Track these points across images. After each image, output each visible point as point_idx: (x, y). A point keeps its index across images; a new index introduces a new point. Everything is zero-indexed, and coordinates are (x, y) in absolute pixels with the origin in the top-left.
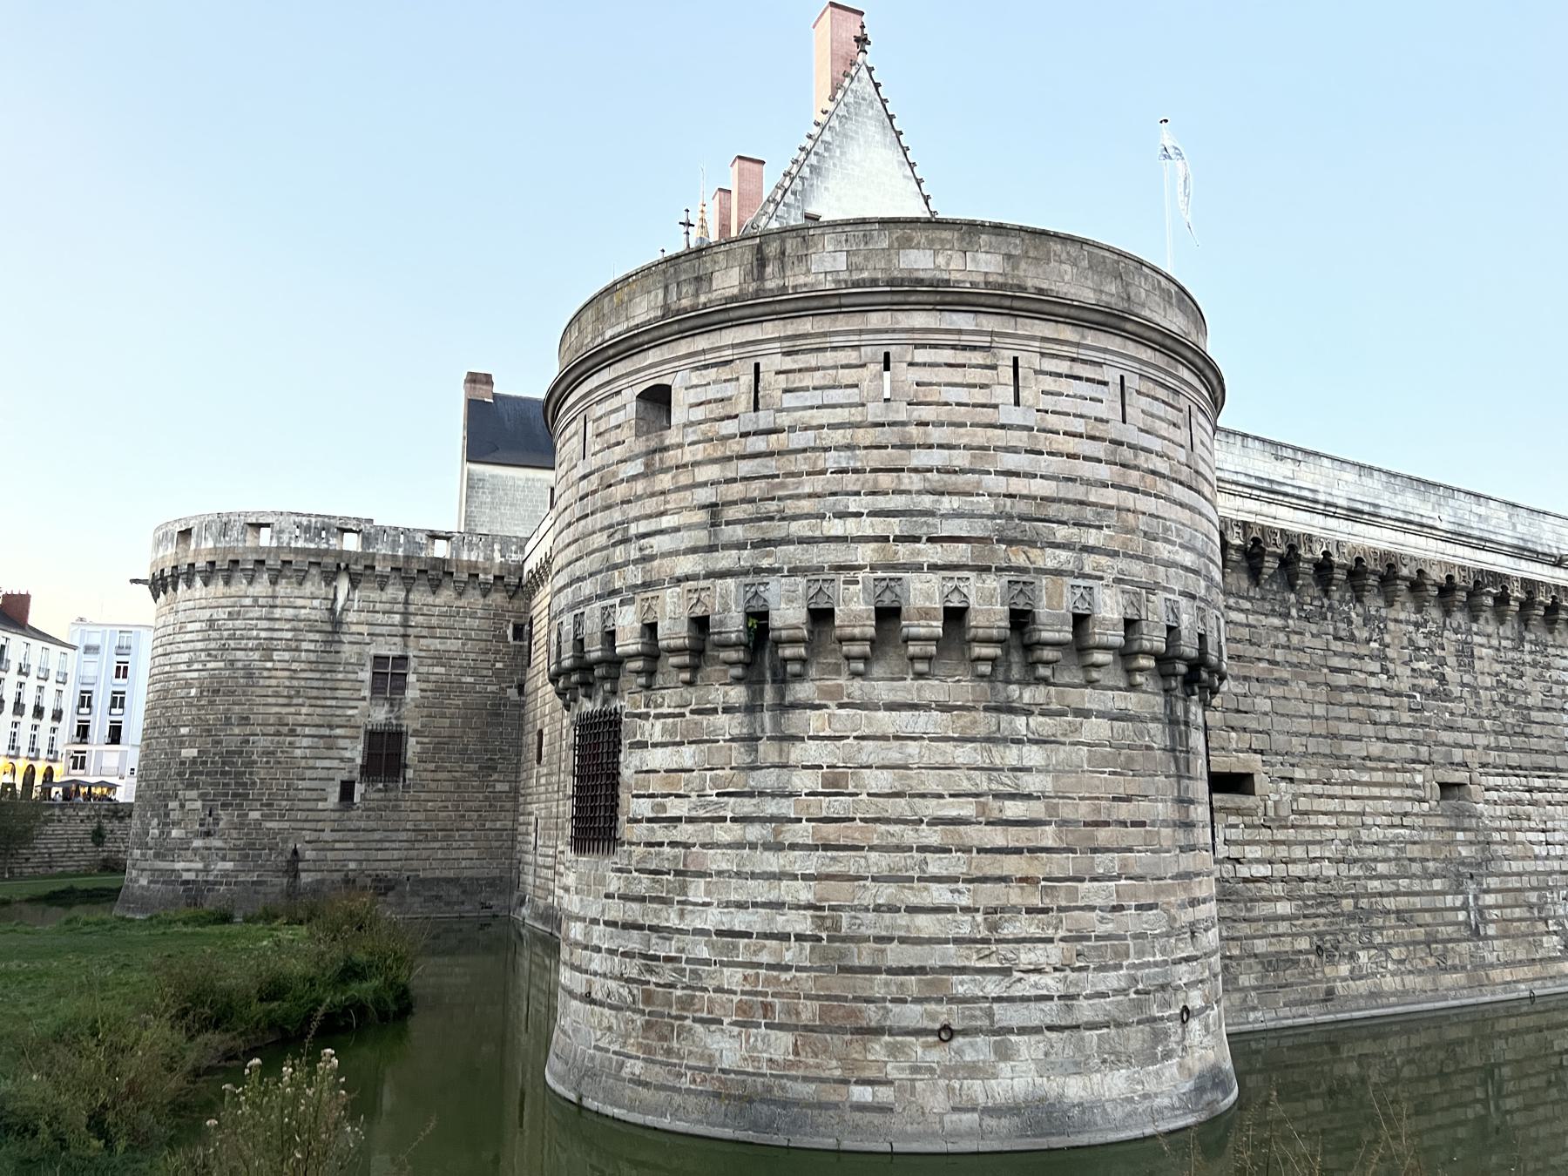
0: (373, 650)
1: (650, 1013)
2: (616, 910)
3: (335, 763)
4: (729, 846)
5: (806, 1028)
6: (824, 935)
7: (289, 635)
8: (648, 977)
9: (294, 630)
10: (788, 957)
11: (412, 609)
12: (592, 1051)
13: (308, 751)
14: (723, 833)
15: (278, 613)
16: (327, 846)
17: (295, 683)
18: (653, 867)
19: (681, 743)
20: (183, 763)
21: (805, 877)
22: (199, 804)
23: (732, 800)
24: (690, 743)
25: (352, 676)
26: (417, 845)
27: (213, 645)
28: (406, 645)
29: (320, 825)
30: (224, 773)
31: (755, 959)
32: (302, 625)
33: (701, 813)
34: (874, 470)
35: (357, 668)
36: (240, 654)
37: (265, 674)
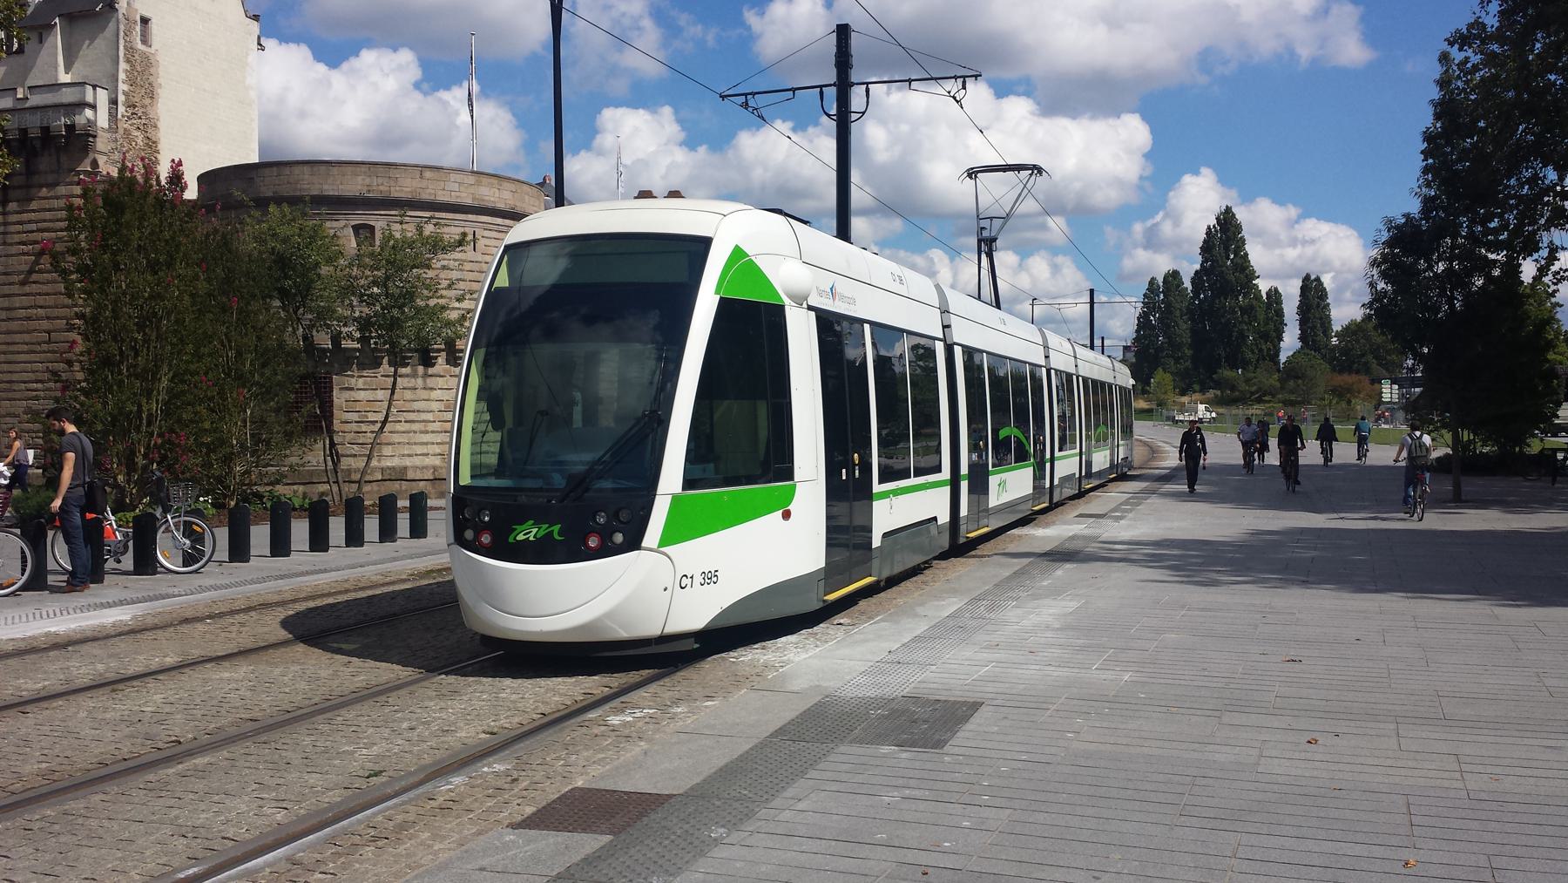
4: (404, 432)
18: (361, 442)
21: (437, 444)
34: (470, 281)
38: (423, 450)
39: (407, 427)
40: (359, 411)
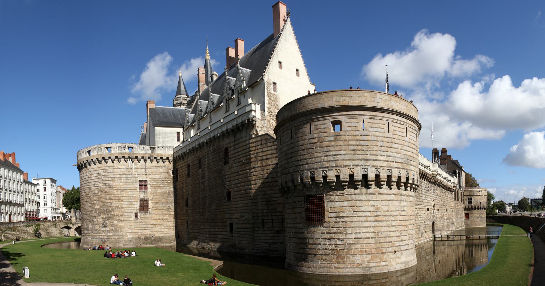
3: (133, 208)
4: (357, 222)
7: (119, 176)
10: (370, 242)
11: (147, 167)
14: (354, 219)
15: (115, 170)
16: (134, 229)
17: (121, 188)
20: (96, 210)
21: (372, 227)
22: (102, 220)
26: (154, 228)
27: (100, 180)
28: (146, 178)
29: (131, 224)
30: (107, 212)
31: (363, 242)
35: (135, 184)
36: (107, 182)
37: (114, 186)
38: (366, 230)
39: (359, 219)
40: (336, 212)
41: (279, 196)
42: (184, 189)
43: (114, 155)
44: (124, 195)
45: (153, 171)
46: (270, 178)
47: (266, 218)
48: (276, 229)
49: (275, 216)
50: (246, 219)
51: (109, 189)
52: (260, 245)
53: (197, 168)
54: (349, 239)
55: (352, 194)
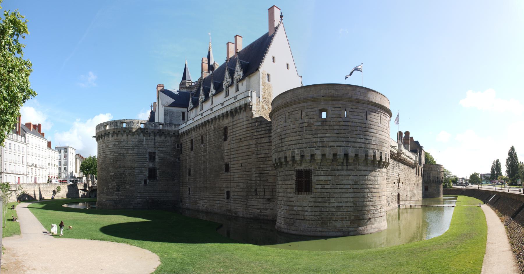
0: (149, 151)
1: (323, 221)
2: (312, 204)
3: (143, 176)
4: (339, 193)
5: (352, 220)
6: (355, 206)
7: (132, 148)
8: (322, 215)
9: (132, 146)
10: (349, 210)
11: (156, 141)
12: (307, 228)
13: (137, 173)
14: (337, 191)
15: (129, 143)
17: (134, 158)
19: (328, 176)
20: (111, 176)
21: (352, 197)
23: (339, 185)
24: (330, 175)
25: (145, 156)
26: (160, 193)
28: (155, 150)
29: (141, 189)
30: (120, 178)
31: (344, 210)
32: (134, 145)
33: (333, 188)
36: (122, 152)
37: (127, 156)
40: (321, 185)
41: (270, 169)
42: (188, 160)
43: (128, 129)
44: (136, 164)
45: (161, 144)
46: (263, 154)
47: (259, 187)
48: (267, 197)
49: (267, 186)
50: (241, 188)
51: (123, 158)
52: (253, 210)
53: (199, 143)
54: (332, 207)
55: (335, 170)
